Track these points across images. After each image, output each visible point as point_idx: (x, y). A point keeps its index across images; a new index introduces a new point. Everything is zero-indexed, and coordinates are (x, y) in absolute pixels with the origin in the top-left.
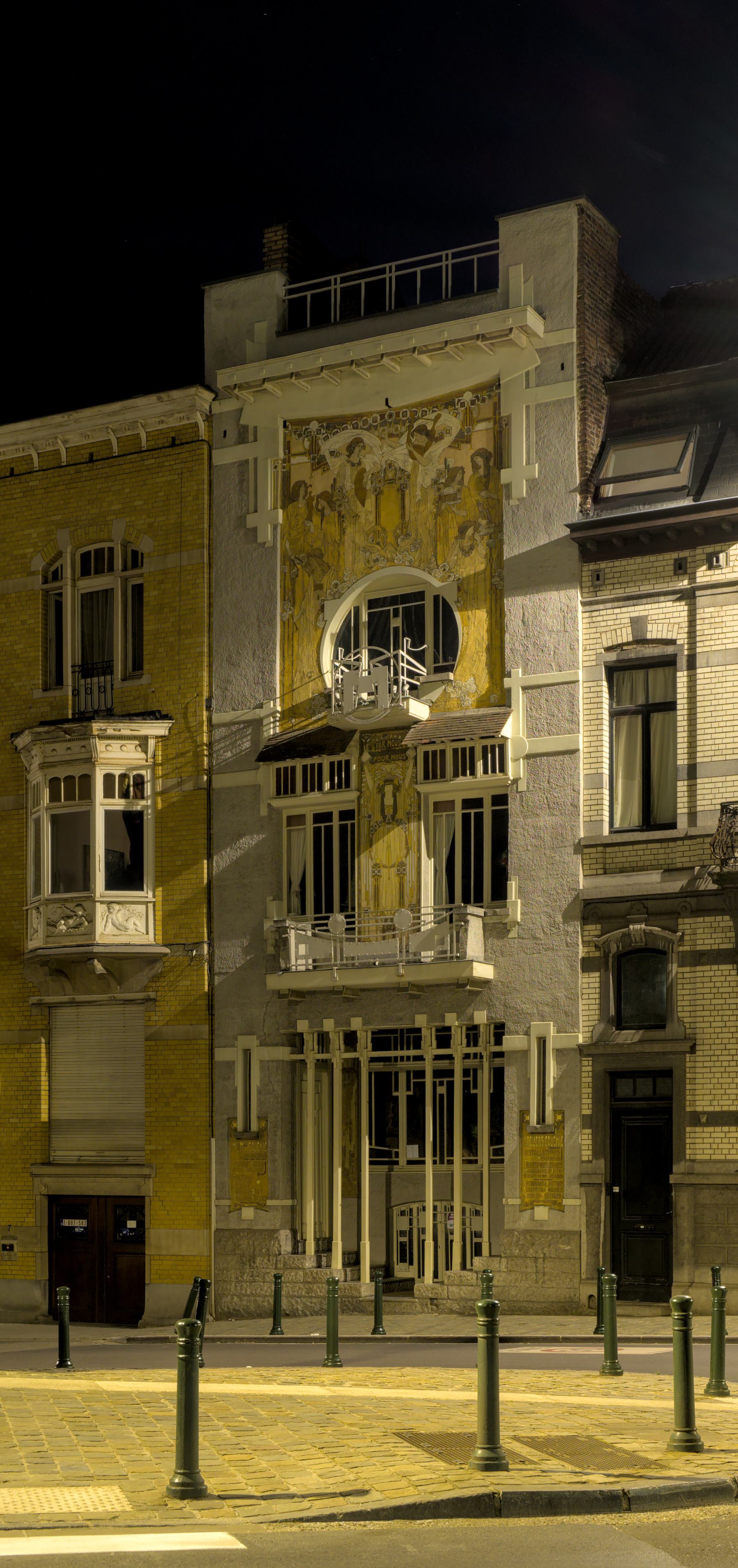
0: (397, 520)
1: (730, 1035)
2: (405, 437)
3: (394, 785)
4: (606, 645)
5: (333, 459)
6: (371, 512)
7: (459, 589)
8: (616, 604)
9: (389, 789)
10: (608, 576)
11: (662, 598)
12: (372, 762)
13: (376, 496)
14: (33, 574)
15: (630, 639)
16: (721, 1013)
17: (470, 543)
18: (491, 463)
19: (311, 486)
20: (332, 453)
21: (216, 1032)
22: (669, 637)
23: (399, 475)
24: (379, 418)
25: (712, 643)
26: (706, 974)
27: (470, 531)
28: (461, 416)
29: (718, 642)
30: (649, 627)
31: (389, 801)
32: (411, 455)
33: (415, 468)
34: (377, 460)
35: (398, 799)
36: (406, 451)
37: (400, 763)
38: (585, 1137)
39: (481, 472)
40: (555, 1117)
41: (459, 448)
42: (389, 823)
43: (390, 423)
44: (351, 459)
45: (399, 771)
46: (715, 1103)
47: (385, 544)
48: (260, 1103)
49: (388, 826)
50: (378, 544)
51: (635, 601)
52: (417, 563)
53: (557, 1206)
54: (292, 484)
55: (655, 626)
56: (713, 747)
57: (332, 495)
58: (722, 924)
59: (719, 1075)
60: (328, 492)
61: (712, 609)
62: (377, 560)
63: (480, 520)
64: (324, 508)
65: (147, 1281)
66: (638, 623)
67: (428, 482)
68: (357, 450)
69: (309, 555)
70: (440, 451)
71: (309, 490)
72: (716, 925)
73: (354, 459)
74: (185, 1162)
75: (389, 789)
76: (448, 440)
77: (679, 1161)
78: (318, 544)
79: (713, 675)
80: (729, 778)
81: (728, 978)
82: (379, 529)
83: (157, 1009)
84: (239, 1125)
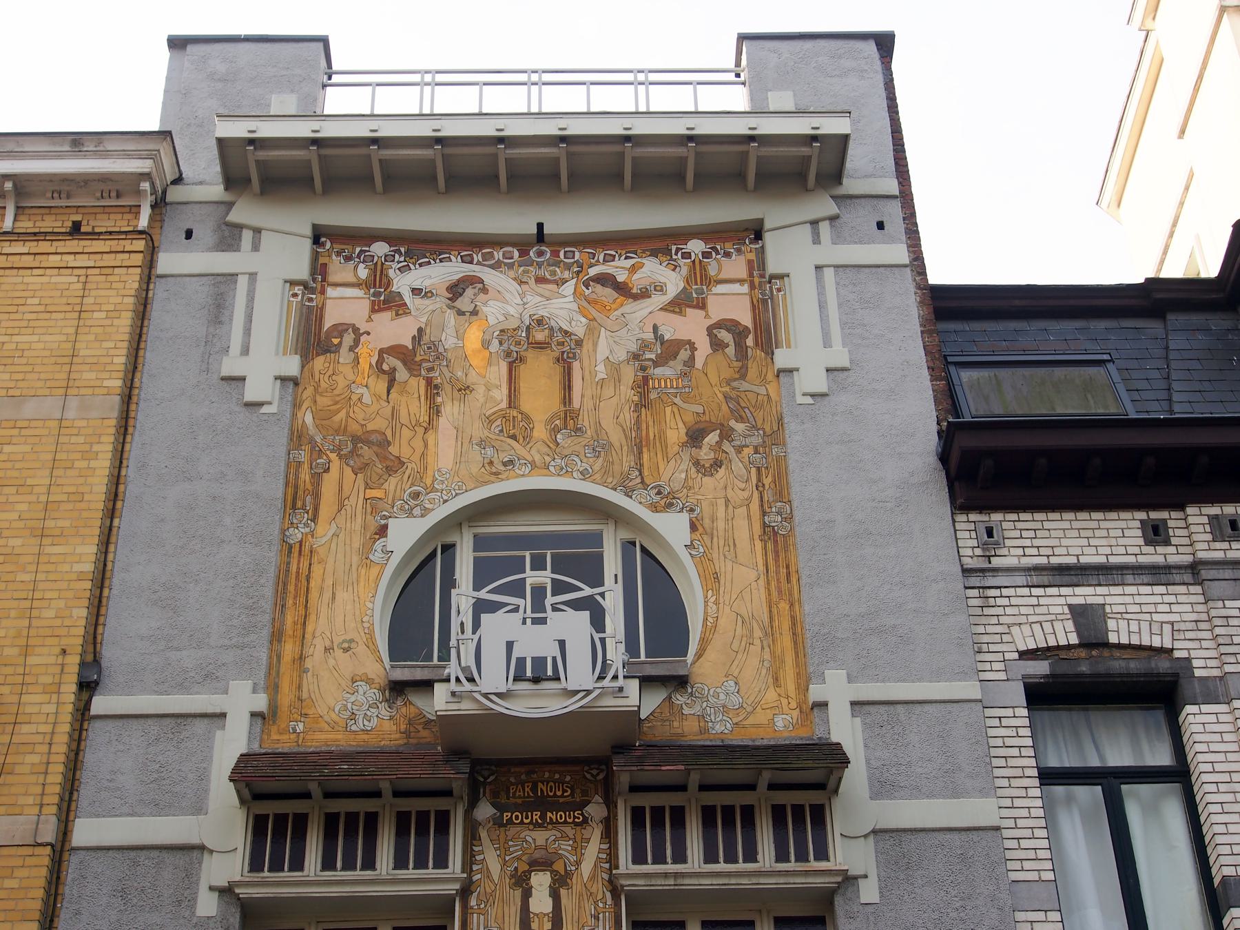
0: (555, 405)
2: (569, 288)
3: (554, 873)
4: (1022, 648)
5: (418, 301)
6: (499, 387)
7: (693, 527)
8: (1035, 580)
9: (541, 882)
10: (1007, 534)
11: (1129, 579)
12: (498, 823)
13: (511, 364)
15: (1074, 639)
17: (712, 455)
18: (750, 341)
19: (368, 333)
20: (416, 291)
22: (1156, 642)
23: (559, 337)
24: (516, 254)
27: (712, 438)
30: (1111, 624)
31: (541, 903)
32: (582, 311)
33: (593, 328)
34: (512, 311)
35: (564, 901)
36: (574, 306)
37: (569, 830)
39: (731, 350)
41: (680, 313)
44: (458, 304)
45: (565, 847)
47: (527, 438)
50: (514, 437)
51: (1075, 579)
52: (598, 477)
54: (325, 329)
60: (407, 347)
62: (509, 463)
63: (732, 423)
64: (394, 370)
67: (622, 356)
68: (469, 292)
69: (356, 439)
70: (645, 312)
71: (363, 338)
73: (464, 303)
75: (541, 882)
76: (658, 300)
78: (379, 424)
82: (515, 415)
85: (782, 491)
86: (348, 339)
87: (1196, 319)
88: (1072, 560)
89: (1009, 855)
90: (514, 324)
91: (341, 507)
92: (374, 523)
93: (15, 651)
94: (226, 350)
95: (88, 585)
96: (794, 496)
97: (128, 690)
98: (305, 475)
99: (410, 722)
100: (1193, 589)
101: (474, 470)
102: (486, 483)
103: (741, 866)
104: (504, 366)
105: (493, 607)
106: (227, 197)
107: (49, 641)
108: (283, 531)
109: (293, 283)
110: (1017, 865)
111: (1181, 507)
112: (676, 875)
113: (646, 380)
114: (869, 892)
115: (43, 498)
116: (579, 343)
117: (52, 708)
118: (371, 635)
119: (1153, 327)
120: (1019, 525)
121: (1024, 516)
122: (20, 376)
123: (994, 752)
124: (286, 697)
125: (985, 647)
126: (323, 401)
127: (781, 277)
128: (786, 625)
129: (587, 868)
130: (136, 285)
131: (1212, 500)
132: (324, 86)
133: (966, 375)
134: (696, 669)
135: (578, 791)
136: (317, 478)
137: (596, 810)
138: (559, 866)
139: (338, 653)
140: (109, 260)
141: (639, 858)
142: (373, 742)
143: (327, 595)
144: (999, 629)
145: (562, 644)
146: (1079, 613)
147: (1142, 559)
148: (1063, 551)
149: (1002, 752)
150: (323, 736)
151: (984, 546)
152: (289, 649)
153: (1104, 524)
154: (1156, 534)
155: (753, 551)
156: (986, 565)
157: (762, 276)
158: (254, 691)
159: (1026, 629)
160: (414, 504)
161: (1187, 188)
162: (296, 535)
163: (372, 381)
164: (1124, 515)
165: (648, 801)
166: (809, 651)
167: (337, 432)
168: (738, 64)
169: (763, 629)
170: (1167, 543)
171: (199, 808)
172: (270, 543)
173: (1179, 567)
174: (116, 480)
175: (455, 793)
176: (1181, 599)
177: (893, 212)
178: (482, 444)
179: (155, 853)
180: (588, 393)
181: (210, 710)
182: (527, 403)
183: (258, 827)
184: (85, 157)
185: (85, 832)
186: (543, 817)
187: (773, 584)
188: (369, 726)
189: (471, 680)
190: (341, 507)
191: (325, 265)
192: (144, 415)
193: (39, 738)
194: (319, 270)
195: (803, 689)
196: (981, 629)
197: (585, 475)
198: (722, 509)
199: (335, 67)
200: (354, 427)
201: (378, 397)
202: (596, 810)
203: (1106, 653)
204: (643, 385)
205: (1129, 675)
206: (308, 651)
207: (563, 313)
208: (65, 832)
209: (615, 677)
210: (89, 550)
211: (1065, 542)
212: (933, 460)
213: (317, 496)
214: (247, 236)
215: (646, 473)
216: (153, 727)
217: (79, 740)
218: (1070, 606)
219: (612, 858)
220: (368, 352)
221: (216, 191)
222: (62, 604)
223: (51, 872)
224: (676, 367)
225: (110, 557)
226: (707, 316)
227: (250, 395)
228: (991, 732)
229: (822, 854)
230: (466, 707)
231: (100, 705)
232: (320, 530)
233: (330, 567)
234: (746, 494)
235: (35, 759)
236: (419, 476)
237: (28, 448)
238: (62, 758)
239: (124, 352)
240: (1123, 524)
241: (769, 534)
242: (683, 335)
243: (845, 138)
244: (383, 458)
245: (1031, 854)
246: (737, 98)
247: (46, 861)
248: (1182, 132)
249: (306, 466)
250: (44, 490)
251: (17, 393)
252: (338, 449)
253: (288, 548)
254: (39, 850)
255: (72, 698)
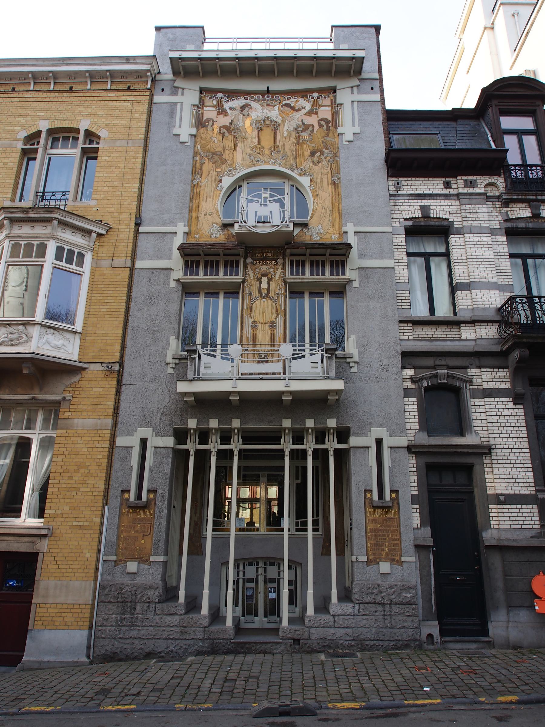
0: (271, 144)
1: (514, 443)
4: (405, 218)
5: (231, 111)
6: (255, 138)
7: (311, 181)
8: (410, 198)
9: (264, 280)
11: (438, 198)
12: (253, 263)
13: (259, 131)
14: (19, 140)
15: (420, 215)
16: (505, 428)
18: (330, 125)
20: (231, 108)
21: (119, 426)
22: (444, 217)
24: (261, 97)
25: (472, 222)
26: (492, 403)
27: (318, 154)
28: (312, 102)
29: (475, 222)
30: (432, 211)
31: (264, 285)
32: (280, 115)
33: (283, 121)
34: (259, 115)
36: (278, 113)
37: (273, 266)
38: (415, 510)
39: (325, 128)
40: (391, 495)
41: (310, 116)
42: (264, 298)
43: (268, 100)
44: (243, 112)
45: (271, 271)
46: (509, 488)
47: (263, 154)
48: (151, 479)
49: (263, 300)
50: (259, 153)
51: (422, 198)
52: (284, 165)
53: (395, 561)
55: (435, 211)
56: (480, 274)
57: (230, 127)
58: (498, 373)
59: (510, 469)
61: (470, 206)
63: (324, 150)
65: (30, 627)
66: (423, 209)
67: (292, 129)
68: (247, 109)
69: (213, 154)
71: (215, 123)
72: (495, 373)
73: (245, 112)
74: (81, 524)
75: (264, 280)
76: (303, 112)
77: (486, 530)
79: (475, 238)
80: (491, 291)
81: (507, 407)
83: (71, 407)
84: (132, 496)
85: (338, 171)
86: (211, 123)
87: (466, 122)
88: (422, 192)
89: (396, 275)
90: (259, 119)
91: (209, 174)
92: (218, 178)
93: (117, 214)
94: (175, 126)
95: (137, 195)
96: (341, 172)
97: (149, 225)
98: (198, 164)
99: (229, 236)
100: (457, 201)
101: (248, 163)
102: (251, 167)
103: (320, 276)
104: (257, 132)
105: (252, 201)
106: (174, 78)
107: (126, 211)
108: (192, 181)
109: (194, 105)
110: (398, 278)
111: (456, 178)
112: (302, 278)
113: (299, 136)
114: (356, 284)
115: (123, 170)
116: (279, 125)
117: (128, 230)
118: (217, 211)
119: (454, 124)
120: (407, 182)
121: (409, 179)
122: (114, 134)
123: (394, 247)
124: (193, 228)
125: (394, 217)
126: (203, 142)
127: (341, 104)
128: (337, 210)
129: (277, 276)
130: (147, 106)
131: (465, 176)
132: (203, 43)
133: (395, 137)
134: (310, 222)
135: (275, 256)
136: (202, 165)
137: (280, 261)
138: (269, 276)
139: (208, 216)
140: (139, 98)
141: (292, 274)
142: (218, 241)
143: (205, 199)
144: (399, 212)
145: (271, 212)
146: (422, 208)
147: (442, 192)
148: (419, 190)
149: (397, 247)
150: (204, 239)
151: (396, 188)
152: (194, 215)
153: (432, 182)
154: (447, 185)
155: (328, 188)
156: (396, 193)
157: (335, 104)
158: (184, 226)
159: (407, 212)
160: (230, 173)
161: (467, 92)
162: (196, 182)
163: (218, 136)
164: (439, 179)
165: (295, 258)
166: (343, 217)
167: (207, 151)
168: (331, 36)
169: (330, 211)
170: (451, 188)
171: (170, 258)
172: (188, 184)
173: (453, 195)
174: (144, 165)
175: (241, 254)
176: (453, 204)
177: (376, 84)
178: (250, 155)
179: (158, 270)
180: (282, 140)
181: (172, 231)
182: (263, 143)
183: (186, 264)
184: (130, 64)
185: (139, 264)
186: (265, 262)
187: (334, 198)
188: (217, 236)
189: (245, 222)
190: (209, 174)
191: (203, 100)
192: (151, 146)
193: (125, 238)
194: (201, 101)
195: (341, 228)
196: (393, 212)
197: (280, 165)
198: (320, 176)
199: (206, 37)
200: (212, 150)
201: (219, 141)
202: (280, 261)
203: (429, 220)
204: (298, 138)
205: (435, 226)
206: (200, 215)
207: (275, 116)
208: (133, 264)
209: (286, 222)
210: (137, 185)
211: (420, 187)
212: (383, 162)
213: (202, 170)
214: (180, 90)
215: (298, 164)
216: (157, 236)
217: (136, 239)
218: (420, 206)
219: (285, 274)
220: (216, 128)
221: (170, 76)
222: (129, 201)
223: (130, 275)
224: (308, 132)
225: (143, 187)
226: (318, 117)
227: (182, 140)
228: (394, 241)
229: (343, 274)
230: (244, 230)
231: (141, 229)
232: (203, 180)
233: (206, 191)
234: (327, 171)
235: (124, 244)
236: (231, 165)
237: (118, 155)
238: (131, 244)
239: (145, 126)
240: (438, 182)
241: (333, 183)
242: (310, 123)
243: (363, 58)
244: (221, 159)
245: (403, 275)
246: (331, 46)
247: (128, 272)
248: (468, 72)
249: (198, 161)
250: (123, 167)
251: (114, 139)
252: (207, 157)
253: (193, 186)
254: (126, 269)
255: (133, 227)
